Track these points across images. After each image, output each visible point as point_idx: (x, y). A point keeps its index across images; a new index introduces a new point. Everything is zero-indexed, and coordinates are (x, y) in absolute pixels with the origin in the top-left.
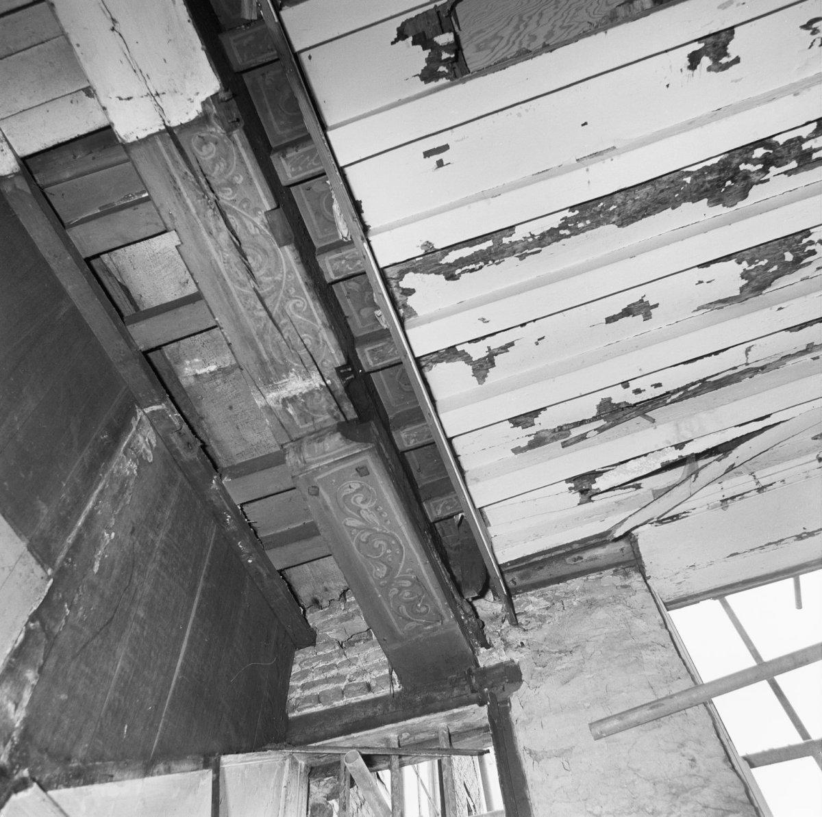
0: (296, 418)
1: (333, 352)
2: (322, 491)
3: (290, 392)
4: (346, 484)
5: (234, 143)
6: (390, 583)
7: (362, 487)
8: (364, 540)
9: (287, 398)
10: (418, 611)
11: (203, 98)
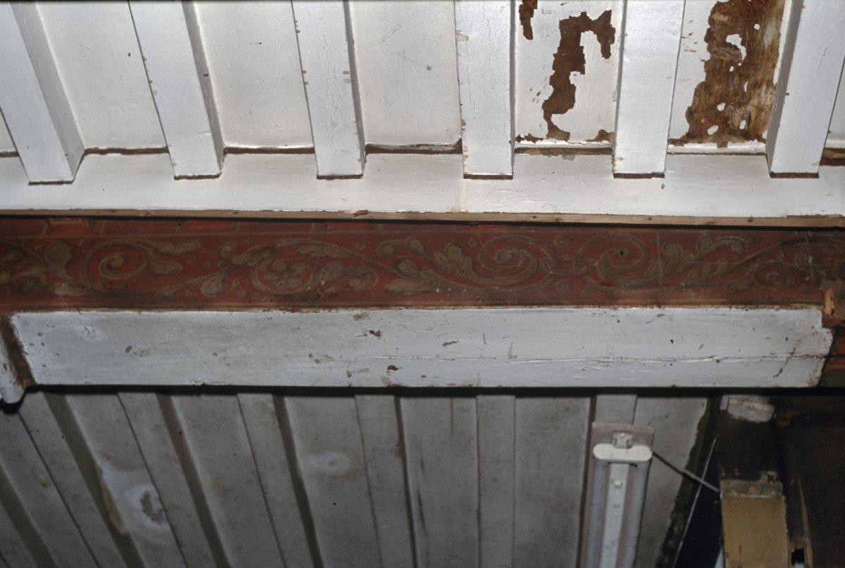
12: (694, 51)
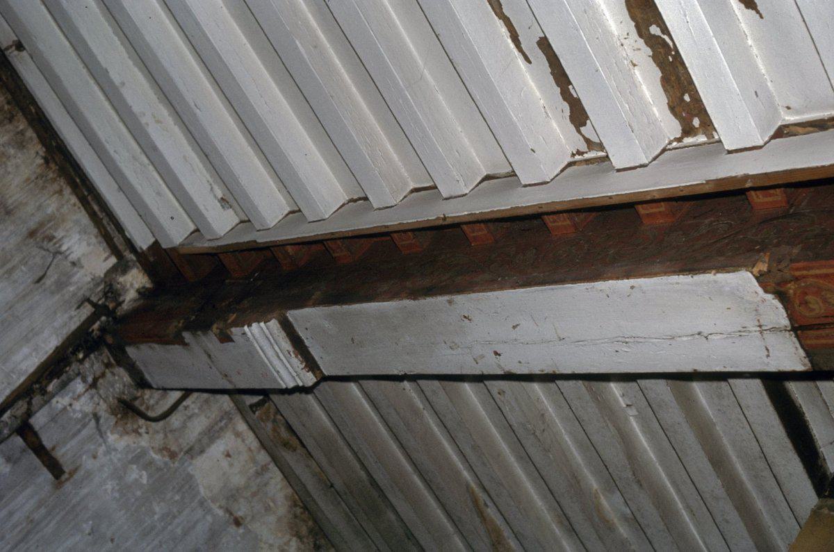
5: (804, 277)
11: (760, 290)
12: (639, 49)
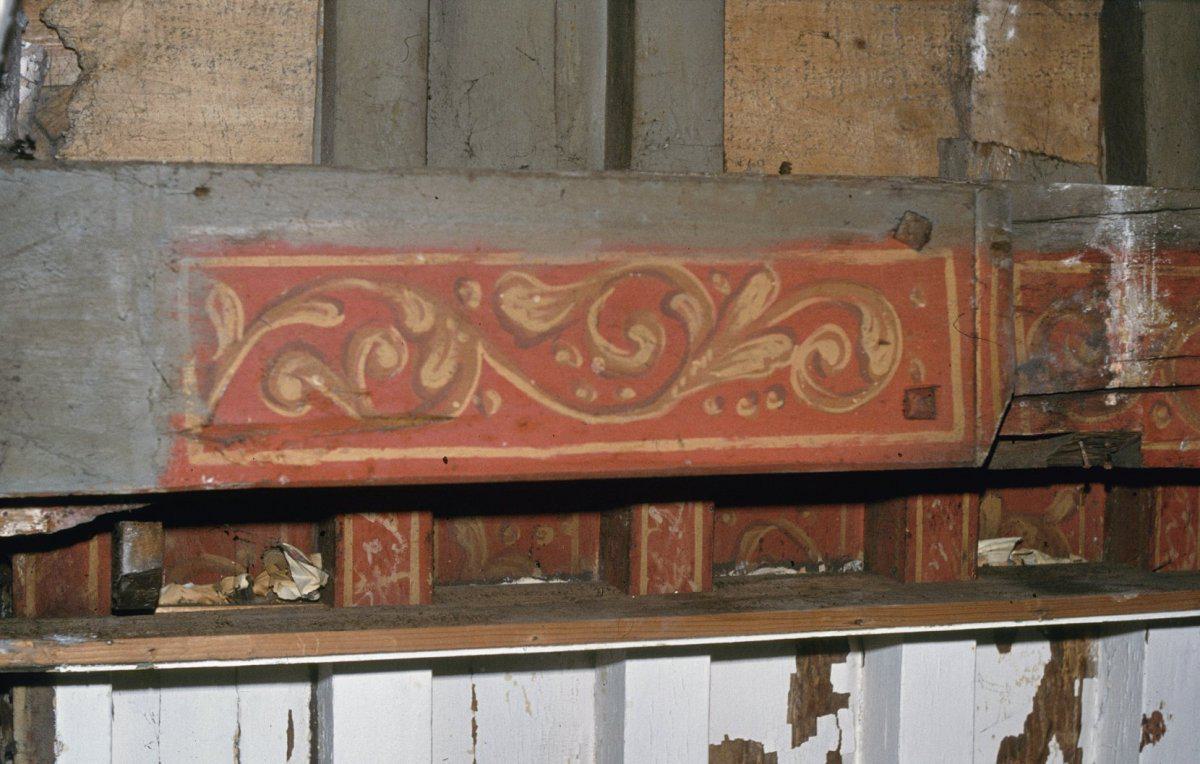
0: (1047, 266)
1: (1183, 447)
2: (909, 254)
3: (1121, 286)
4: (896, 334)
6: (465, 318)
7: (868, 379)
8: (677, 302)
9: (1109, 271)
10: (293, 365)
